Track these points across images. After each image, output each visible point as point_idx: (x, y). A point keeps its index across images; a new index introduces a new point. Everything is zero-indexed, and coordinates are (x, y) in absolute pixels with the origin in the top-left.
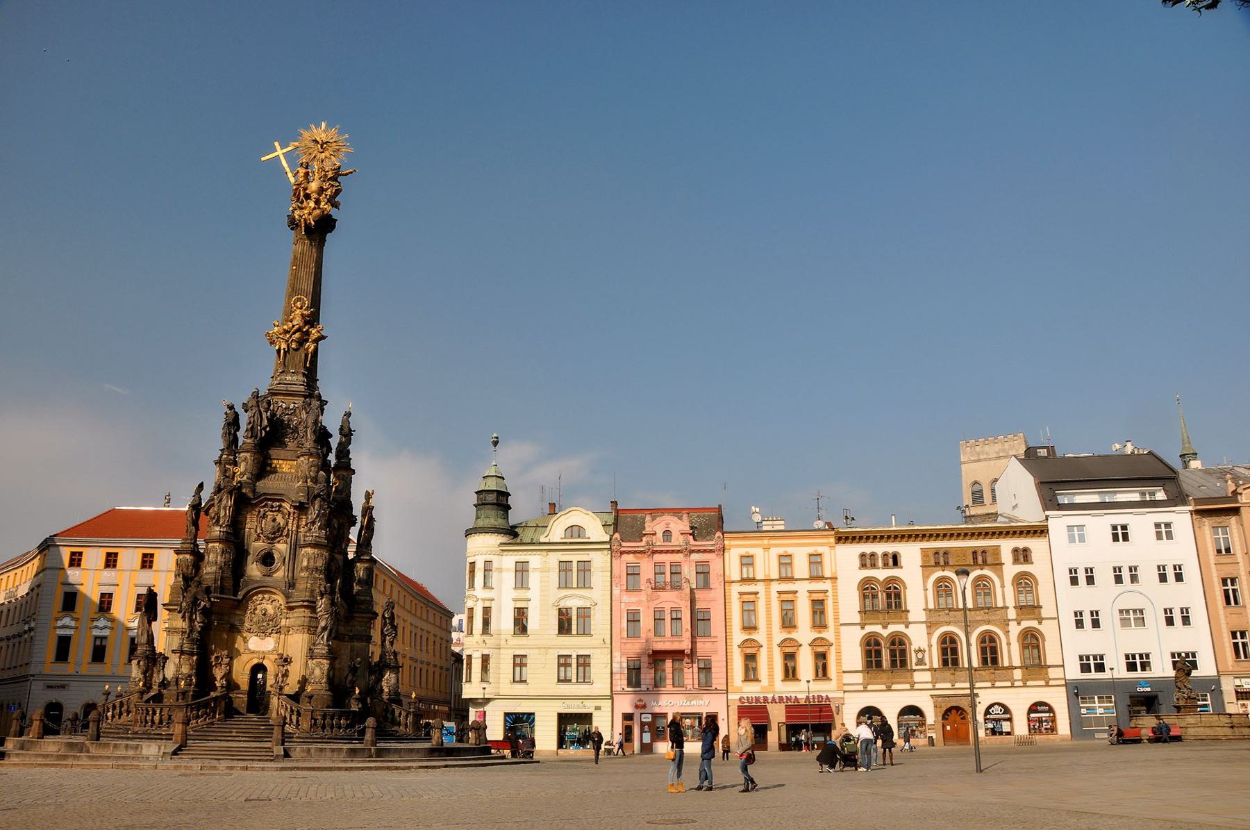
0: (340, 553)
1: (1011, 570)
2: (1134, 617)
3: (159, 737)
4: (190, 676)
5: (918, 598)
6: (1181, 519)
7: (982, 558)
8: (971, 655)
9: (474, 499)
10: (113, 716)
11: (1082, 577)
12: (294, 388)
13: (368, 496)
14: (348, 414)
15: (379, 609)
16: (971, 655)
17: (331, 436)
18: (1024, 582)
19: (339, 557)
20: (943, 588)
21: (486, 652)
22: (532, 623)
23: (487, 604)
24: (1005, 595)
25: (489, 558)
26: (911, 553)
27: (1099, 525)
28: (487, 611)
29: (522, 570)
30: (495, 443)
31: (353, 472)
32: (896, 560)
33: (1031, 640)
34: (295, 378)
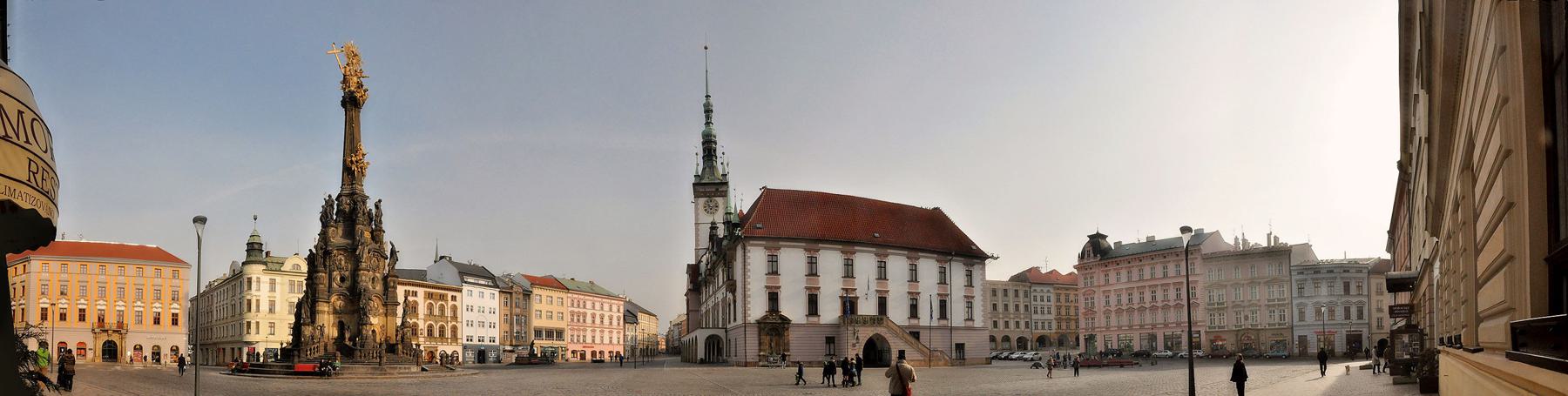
1: (450, 303)
2: (482, 324)
5: (422, 310)
6: (496, 292)
7: (442, 297)
8: (436, 333)
11: (470, 309)
16: (436, 333)
18: (454, 308)
20: (430, 307)
22: (277, 308)
24: (448, 313)
26: (421, 291)
27: (476, 290)
29: (273, 282)
32: (415, 294)
33: (454, 329)
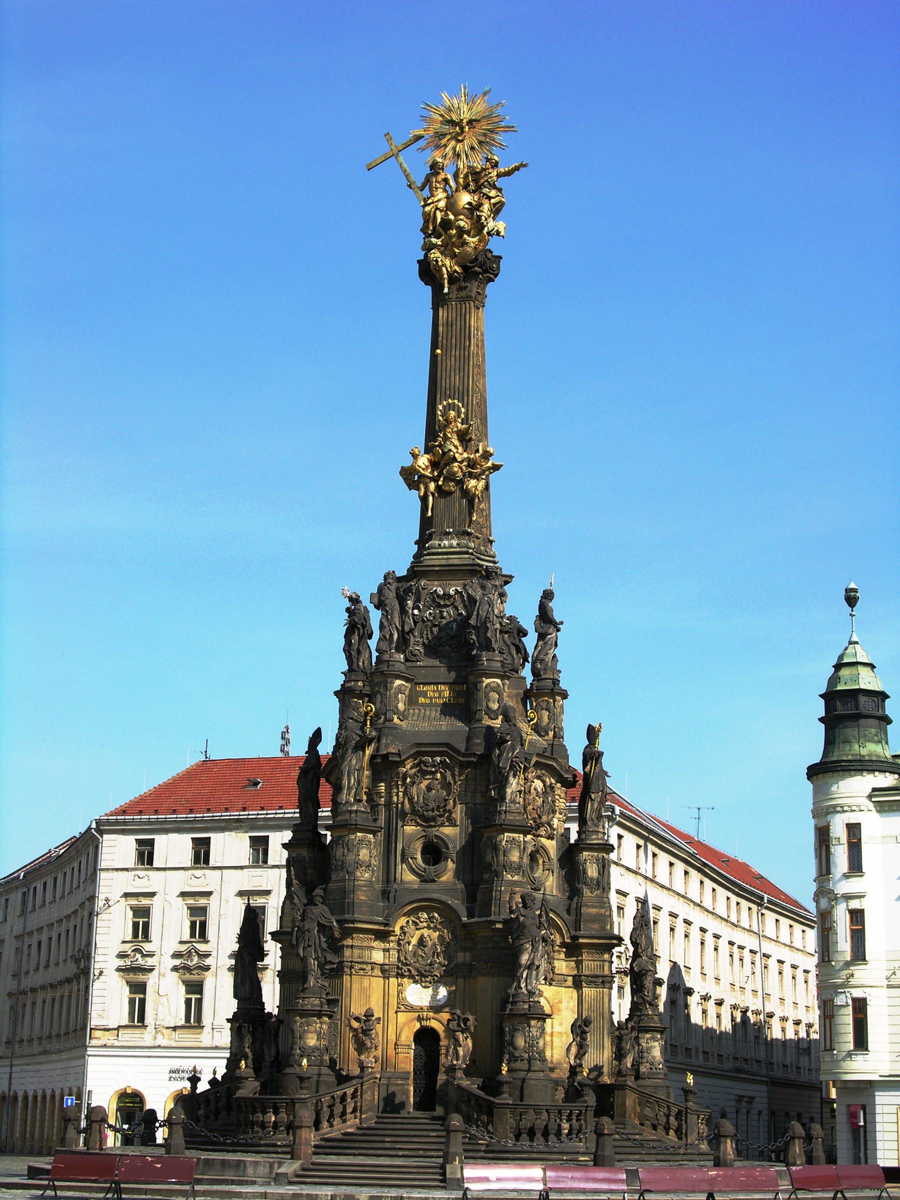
0: (550, 837)
3: (271, 1149)
4: (315, 1049)
9: (820, 709)
10: (207, 1117)
12: (455, 560)
13: (592, 733)
14: (548, 595)
15: (624, 926)
17: (525, 634)
19: (551, 845)
21: (857, 993)
23: (854, 904)
25: (853, 818)
28: (857, 916)
30: (851, 599)
31: (565, 695)
34: (455, 542)
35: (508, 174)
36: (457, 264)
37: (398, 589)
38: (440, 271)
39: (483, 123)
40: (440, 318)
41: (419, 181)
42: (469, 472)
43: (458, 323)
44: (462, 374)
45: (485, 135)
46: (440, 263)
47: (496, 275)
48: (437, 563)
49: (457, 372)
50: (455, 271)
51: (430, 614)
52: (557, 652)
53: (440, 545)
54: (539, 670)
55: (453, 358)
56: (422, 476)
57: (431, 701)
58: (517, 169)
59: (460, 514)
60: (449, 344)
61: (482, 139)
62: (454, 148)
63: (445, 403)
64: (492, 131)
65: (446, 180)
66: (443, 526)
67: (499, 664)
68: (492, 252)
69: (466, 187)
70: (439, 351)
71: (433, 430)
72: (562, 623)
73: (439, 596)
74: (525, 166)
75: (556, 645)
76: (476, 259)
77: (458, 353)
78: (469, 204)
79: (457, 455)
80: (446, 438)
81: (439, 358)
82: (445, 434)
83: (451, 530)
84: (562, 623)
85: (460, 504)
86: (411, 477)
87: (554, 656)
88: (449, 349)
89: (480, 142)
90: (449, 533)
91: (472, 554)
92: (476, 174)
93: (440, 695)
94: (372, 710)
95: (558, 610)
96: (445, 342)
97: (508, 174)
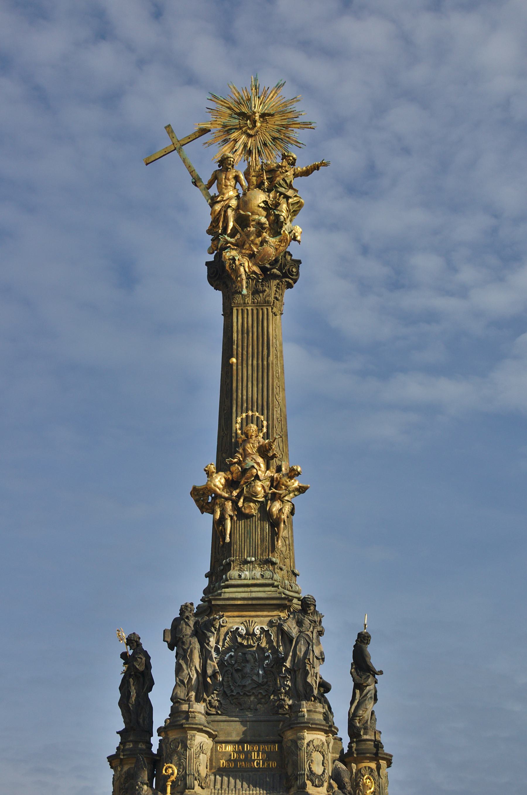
14: (363, 639)
35: (307, 173)
36: (255, 264)
37: (196, 623)
38: (236, 271)
39: (277, 117)
40: (235, 324)
41: (206, 178)
42: (274, 494)
43: (255, 330)
44: (260, 385)
45: (279, 131)
46: (237, 262)
47: (295, 281)
48: (239, 595)
49: (255, 383)
50: (254, 272)
51: (231, 656)
52: (377, 708)
53: (240, 576)
54: (359, 729)
55: (250, 368)
56: (217, 496)
57: (236, 765)
58: (316, 168)
59: (262, 540)
60: (245, 353)
61: (277, 135)
62: (245, 146)
63: (244, 415)
64: (286, 127)
65: (237, 178)
66: (241, 552)
67: (321, 717)
68: (291, 255)
69: (260, 186)
70: (234, 360)
71: (228, 446)
72: (381, 673)
73: (241, 636)
74: (326, 165)
75: (376, 699)
76: (276, 260)
77: (255, 362)
78: (265, 202)
79: (259, 473)
80: (245, 455)
81: (235, 368)
82: (244, 450)
83: (253, 559)
84: (381, 673)
85: (262, 530)
86: (204, 498)
87: (373, 713)
88: (245, 357)
89: (274, 139)
90: (251, 562)
91: (277, 586)
92: (272, 172)
93: (246, 757)
94: (173, 774)
95: (376, 656)
96: (240, 349)
97: (307, 173)
